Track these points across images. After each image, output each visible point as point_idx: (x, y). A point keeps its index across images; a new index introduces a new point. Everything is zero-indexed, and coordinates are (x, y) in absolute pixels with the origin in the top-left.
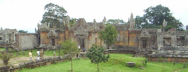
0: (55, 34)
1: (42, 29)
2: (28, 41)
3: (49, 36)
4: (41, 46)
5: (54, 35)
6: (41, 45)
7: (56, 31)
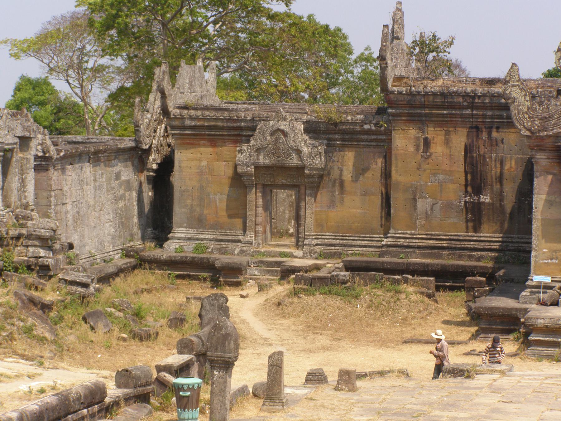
0: (305, 150)
1: (186, 107)
2: (92, 203)
3: (252, 169)
4: (181, 241)
5: (295, 161)
6: (179, 231)
7: (307, 131)
